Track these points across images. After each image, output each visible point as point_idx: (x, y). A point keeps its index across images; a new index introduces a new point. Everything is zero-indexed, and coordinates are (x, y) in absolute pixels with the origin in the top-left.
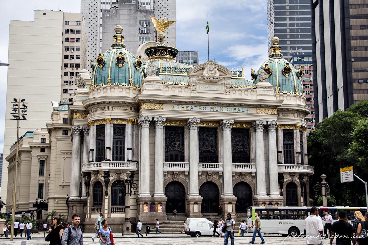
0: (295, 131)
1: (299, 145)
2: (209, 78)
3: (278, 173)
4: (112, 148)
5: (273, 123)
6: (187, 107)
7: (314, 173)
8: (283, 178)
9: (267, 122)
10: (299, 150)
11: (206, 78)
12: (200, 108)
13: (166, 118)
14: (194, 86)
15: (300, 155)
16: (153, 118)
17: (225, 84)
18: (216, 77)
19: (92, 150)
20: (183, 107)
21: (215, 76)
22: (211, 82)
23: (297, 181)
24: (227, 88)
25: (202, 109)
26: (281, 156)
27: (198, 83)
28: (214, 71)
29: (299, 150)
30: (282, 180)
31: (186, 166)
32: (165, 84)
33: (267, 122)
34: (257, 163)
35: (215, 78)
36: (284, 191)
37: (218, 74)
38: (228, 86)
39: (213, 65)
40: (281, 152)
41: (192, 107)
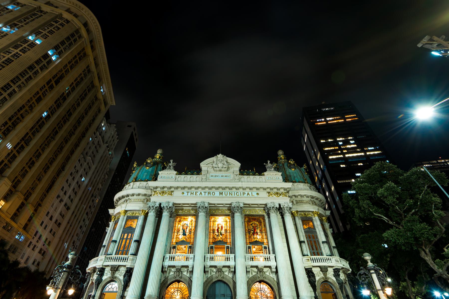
0: (314, 218)
1: (322, 233)
3: (306, 269)
4: (118, 241)
5: (286, 206)
7: (351, 270)
8: (313, 275)
9: (280, 205)
10: (324, 239)
13: (174, 204)
15: (326, 245)
16: (160, 204)
19: (105, 246)
22: (220, 171)
23: (333, 280)
25: (211, 194)
26: (305, 247)
29: (324, 239)
30: (313, 278)
31: (191, 259)
33: (280, 205)
34: (276, 253)
36: (318, 294)
40: (304, 242)
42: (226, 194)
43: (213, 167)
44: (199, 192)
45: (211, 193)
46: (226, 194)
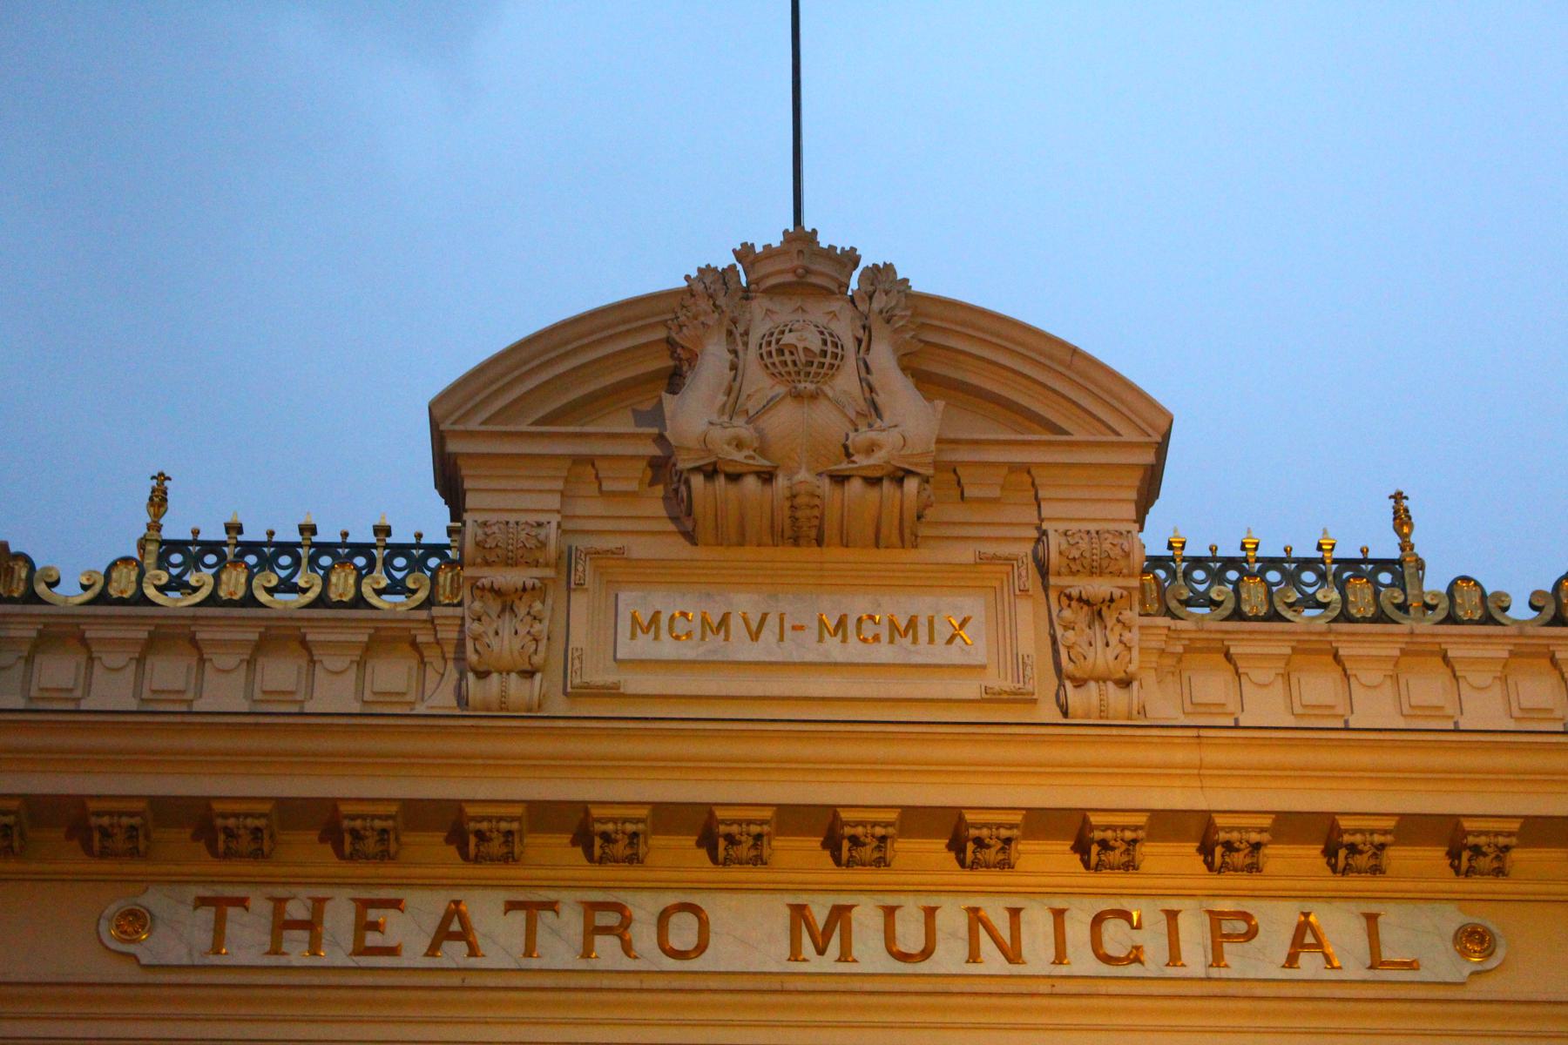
2: (767, 477)
6: (373, 915)
11: (710, 473)
12: (611, 919)
14: (506, 600)
17: (1043, 569)
18: (871, 449)
20: (297, 910)
21: (864, 435)
22: (801, 529)
24: (1082, 616)
25: (644, 935)
27: (584, 570)
28: (846, 382)
32: (32, 597)
35: (861, 460)
37: (911, 420)
38: (1099, 587)
39: (836, 305)
41: (455, 910)
42: (910, 936)
43: (661, 468)
44: (426, 907)
45: (644, 908)
46: (910, 936)
